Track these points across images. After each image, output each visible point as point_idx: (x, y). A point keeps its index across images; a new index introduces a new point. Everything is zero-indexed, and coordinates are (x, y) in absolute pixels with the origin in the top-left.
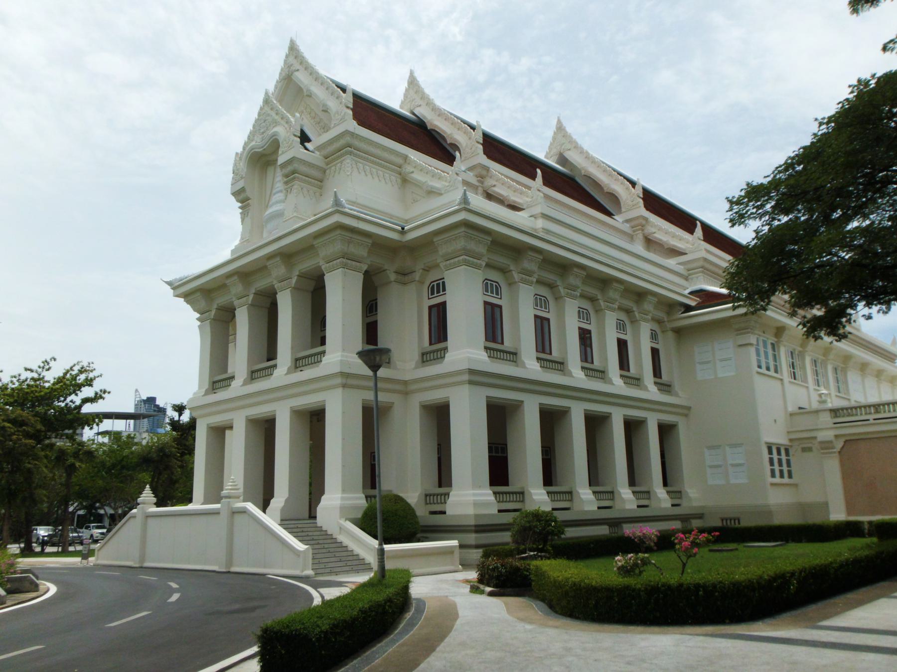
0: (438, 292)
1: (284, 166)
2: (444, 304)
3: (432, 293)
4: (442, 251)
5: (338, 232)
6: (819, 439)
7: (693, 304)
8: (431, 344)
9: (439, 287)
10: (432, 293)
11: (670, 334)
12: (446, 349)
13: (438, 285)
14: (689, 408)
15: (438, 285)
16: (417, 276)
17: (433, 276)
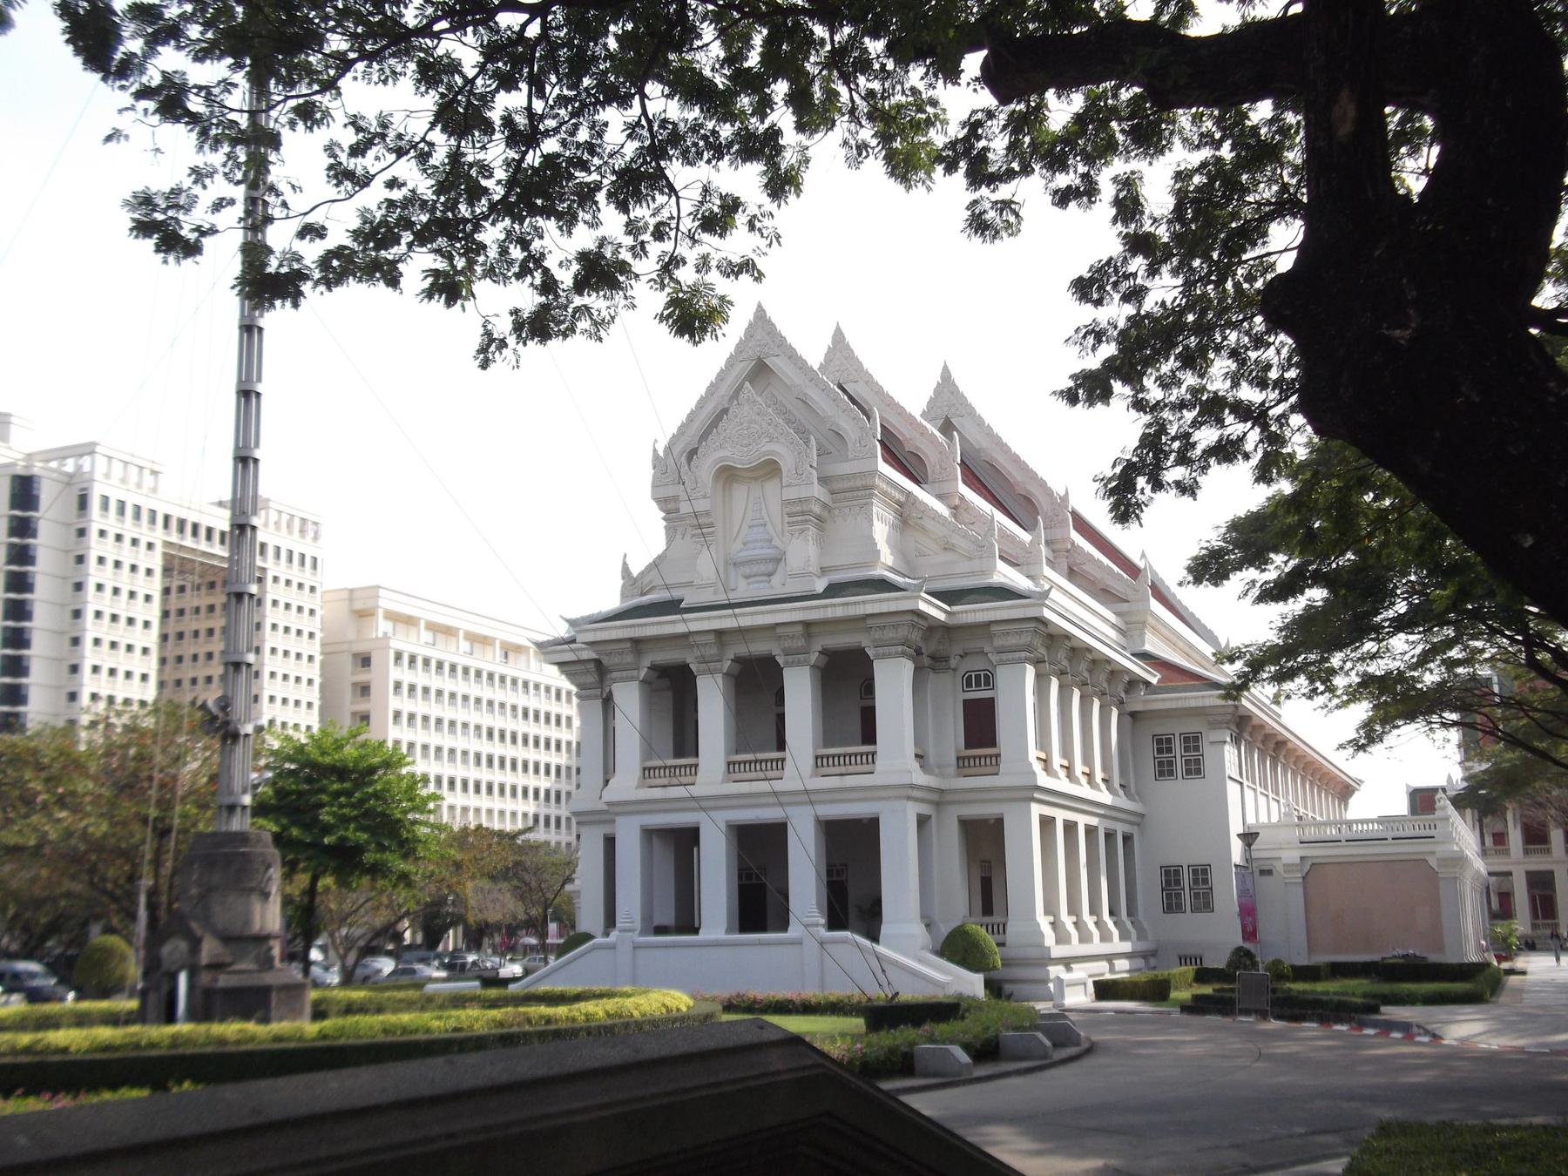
0: (978, 684)
1: (790, 502)
2: (989, 705)
3: (969, 684)
4: (998, 642)
5: (910, 617)
6: (1284, 861)
7: (1154, 681)
8: (968, 745)
9: (988, 680)
10: (969, 684)
11: (1129, 718)
12: (998, 756)
13: (978, 677)
14: (1142, 816)
15: (978, 677)
16: (953, 663)
17: (975, 664)
